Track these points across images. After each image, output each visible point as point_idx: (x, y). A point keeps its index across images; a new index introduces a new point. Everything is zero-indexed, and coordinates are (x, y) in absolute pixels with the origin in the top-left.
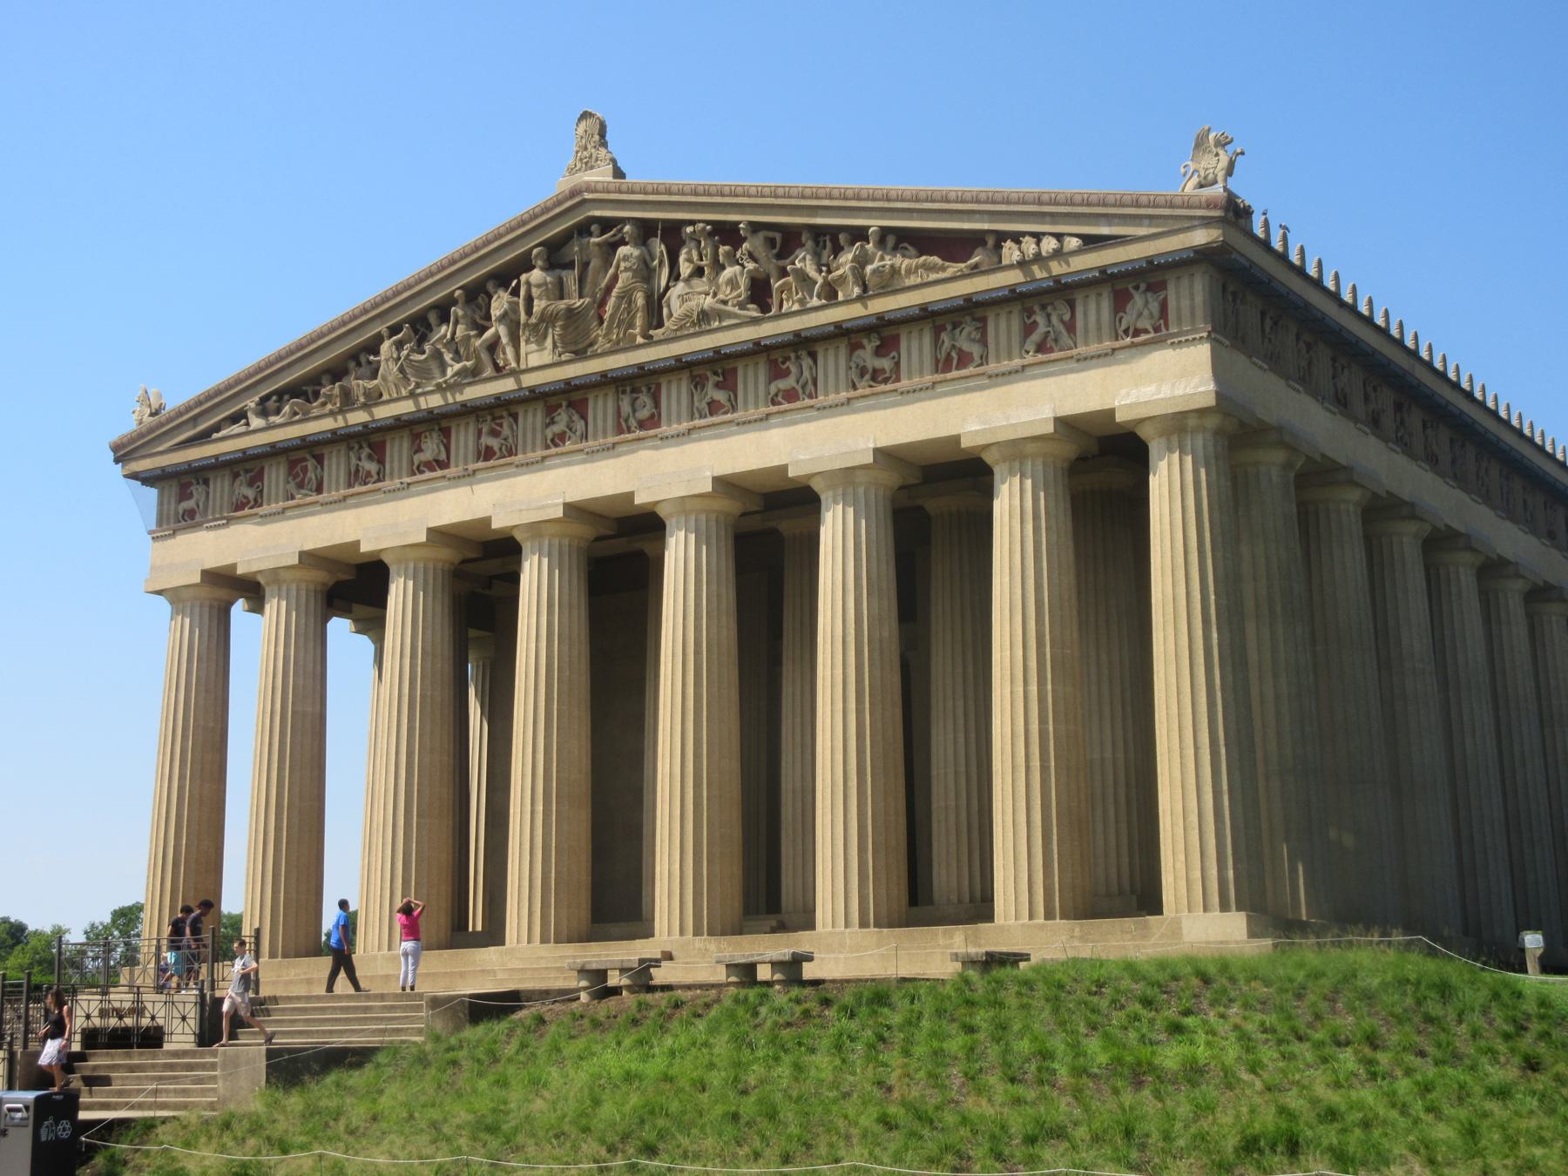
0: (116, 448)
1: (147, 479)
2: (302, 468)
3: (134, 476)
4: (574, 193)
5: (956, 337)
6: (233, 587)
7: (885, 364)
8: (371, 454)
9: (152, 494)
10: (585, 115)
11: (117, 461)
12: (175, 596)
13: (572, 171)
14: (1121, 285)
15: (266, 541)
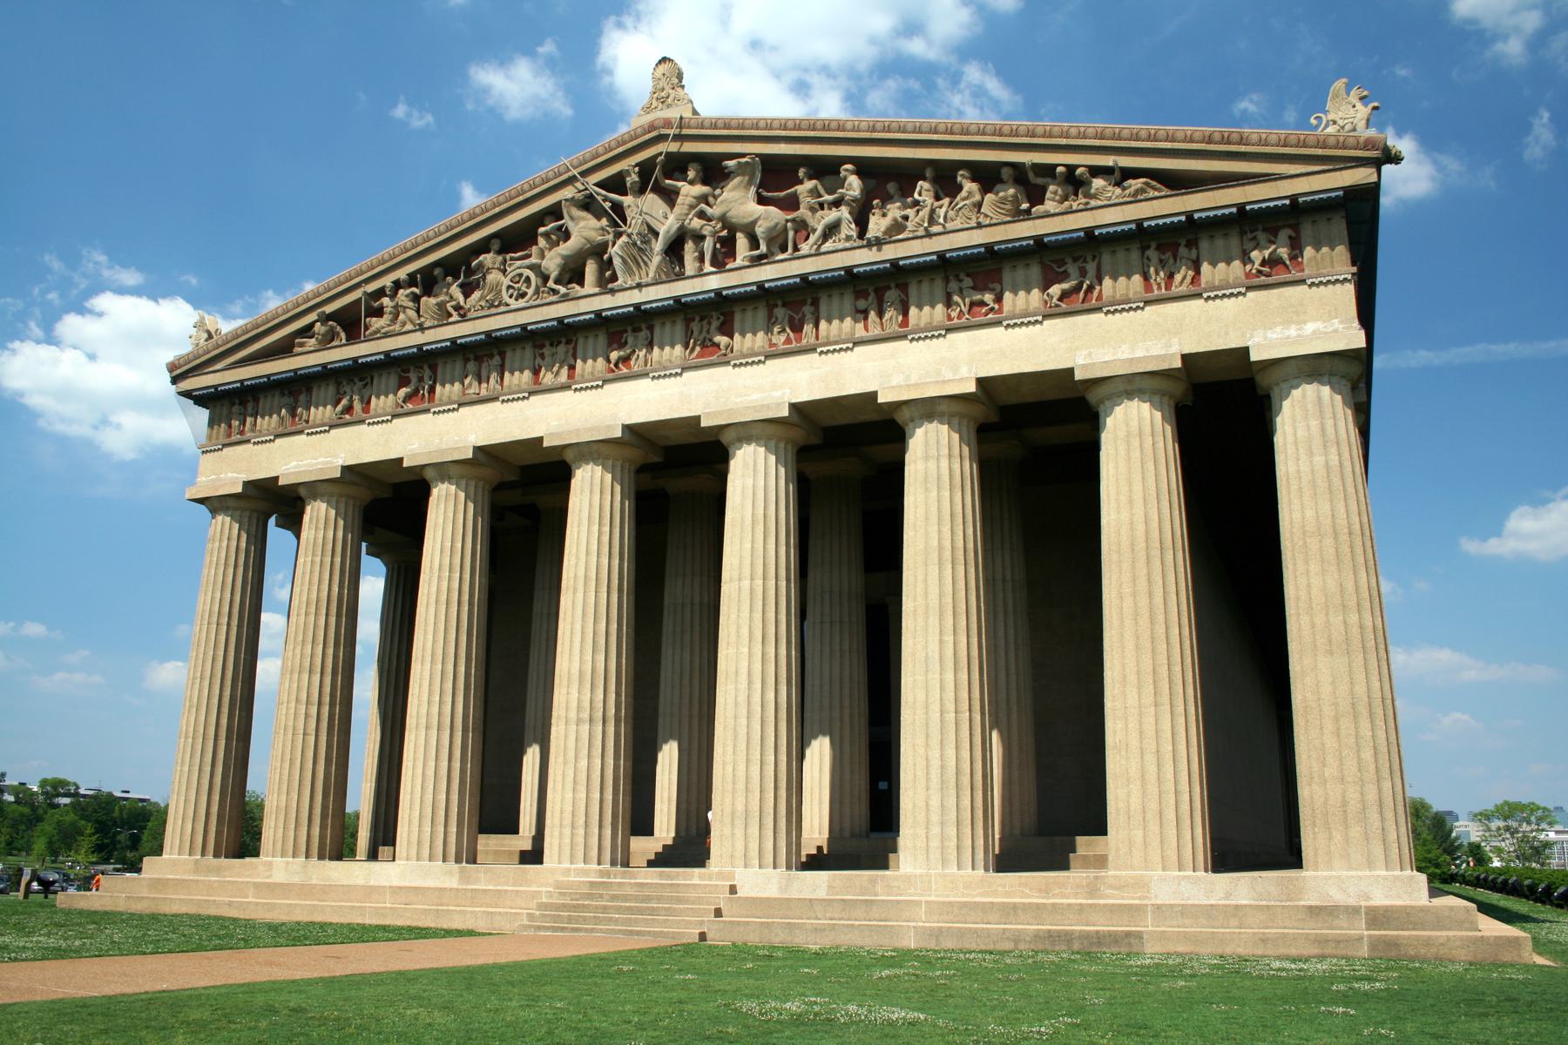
0: (171, 367)
1: (200, 399)
2: (350, 385)
3: (187, 394)
4: (652, 127)
5: (1070, 268)
6: (274, 504)
7: (988, 297)
8: (417, 375)
9: (203, 414)
10: (664, 60)
11: (175, 380)
12: (214, 504)
13: (648, 109)
14: (1248, 225)
15: (311, 453)
